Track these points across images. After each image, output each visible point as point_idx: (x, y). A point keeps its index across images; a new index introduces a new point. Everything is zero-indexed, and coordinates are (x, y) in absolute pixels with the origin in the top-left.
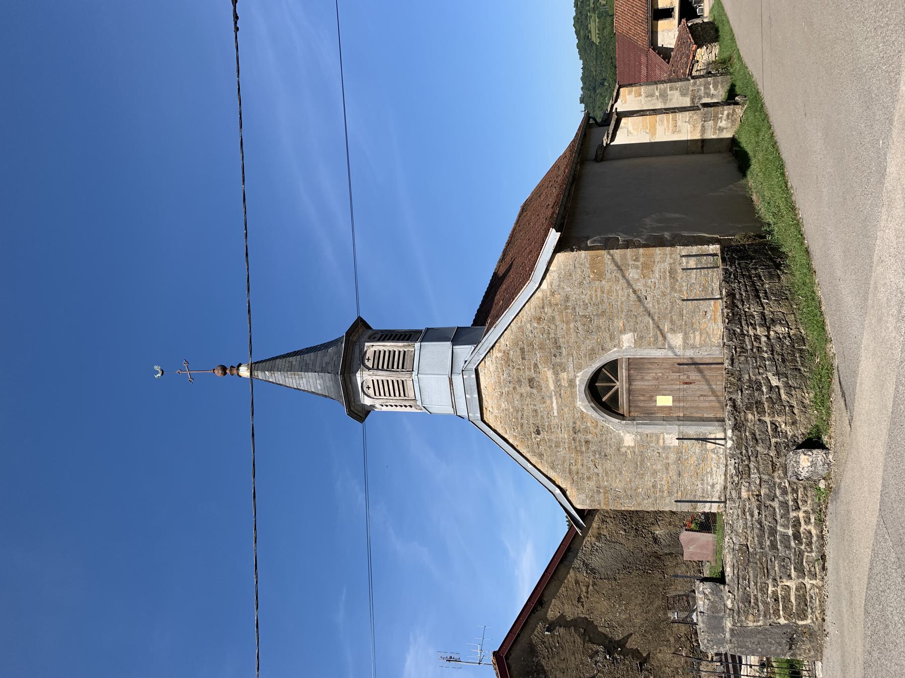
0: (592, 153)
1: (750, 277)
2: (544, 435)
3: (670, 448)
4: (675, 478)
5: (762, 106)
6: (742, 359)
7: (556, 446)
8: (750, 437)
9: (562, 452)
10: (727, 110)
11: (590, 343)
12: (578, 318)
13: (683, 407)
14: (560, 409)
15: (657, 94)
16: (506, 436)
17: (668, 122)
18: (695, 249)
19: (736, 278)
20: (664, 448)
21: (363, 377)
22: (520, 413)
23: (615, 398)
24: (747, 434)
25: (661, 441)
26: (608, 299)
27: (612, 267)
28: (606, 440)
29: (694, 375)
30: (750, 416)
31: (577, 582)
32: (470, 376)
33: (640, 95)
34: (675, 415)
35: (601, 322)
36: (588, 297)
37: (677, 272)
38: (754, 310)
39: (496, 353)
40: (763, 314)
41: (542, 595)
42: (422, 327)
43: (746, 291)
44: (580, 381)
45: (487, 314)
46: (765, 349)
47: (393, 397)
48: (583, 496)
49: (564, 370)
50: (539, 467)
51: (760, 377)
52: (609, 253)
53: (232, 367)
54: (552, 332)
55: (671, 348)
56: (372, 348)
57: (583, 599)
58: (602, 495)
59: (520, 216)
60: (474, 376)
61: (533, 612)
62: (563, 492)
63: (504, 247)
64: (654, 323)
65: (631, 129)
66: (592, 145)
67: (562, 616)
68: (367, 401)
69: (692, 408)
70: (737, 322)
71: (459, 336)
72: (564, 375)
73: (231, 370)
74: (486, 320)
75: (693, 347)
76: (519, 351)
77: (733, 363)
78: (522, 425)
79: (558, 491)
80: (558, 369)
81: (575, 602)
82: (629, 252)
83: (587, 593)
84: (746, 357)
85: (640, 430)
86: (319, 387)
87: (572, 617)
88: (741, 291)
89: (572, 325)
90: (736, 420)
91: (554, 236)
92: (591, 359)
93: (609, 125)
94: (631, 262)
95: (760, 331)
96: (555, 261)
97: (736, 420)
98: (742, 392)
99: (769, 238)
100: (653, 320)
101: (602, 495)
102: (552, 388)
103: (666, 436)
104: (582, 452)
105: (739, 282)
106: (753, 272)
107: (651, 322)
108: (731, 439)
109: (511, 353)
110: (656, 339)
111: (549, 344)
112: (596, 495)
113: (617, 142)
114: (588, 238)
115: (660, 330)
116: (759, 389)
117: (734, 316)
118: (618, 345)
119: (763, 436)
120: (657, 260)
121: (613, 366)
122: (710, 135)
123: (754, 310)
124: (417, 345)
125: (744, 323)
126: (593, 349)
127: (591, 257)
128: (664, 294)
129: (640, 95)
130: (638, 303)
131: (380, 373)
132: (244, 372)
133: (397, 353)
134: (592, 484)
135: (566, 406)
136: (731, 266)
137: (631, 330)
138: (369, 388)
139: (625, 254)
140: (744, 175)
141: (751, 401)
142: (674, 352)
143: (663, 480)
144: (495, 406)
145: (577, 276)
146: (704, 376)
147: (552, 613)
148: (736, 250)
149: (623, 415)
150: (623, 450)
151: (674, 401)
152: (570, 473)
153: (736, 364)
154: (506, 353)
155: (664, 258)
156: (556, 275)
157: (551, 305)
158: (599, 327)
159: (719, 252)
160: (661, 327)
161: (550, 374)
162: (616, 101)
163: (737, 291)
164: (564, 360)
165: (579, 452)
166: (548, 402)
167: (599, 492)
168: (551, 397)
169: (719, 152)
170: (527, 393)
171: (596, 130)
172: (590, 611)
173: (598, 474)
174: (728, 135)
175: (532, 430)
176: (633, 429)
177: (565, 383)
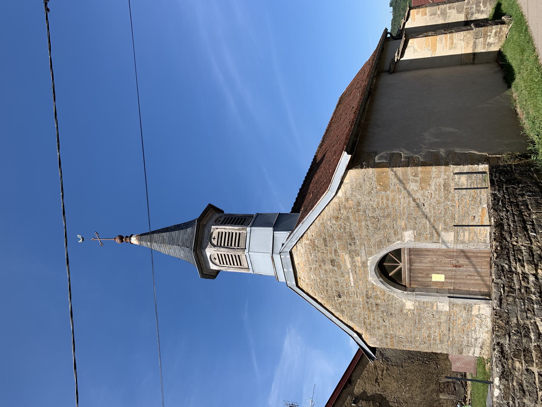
0: (387, 66)
1: (517, 205)
3: (442, 312)
4: (446, 332)
5: (526, 30)
6: (510, 299)
7: (353, 306)
8: (517, 387)
9: (358, 310)
10: (495, 29)
11: (378, 237)
12: (368, 218)
13: (454, 283)
14: (356, 282)
15: (439, 12)
16: (316, 297)
17: (446, 40)
18: (466, 168)
19: (504, 204)
20: (437, 312)
21: (209, 252)
23: (399, 273)
24: (515, 384)
25: (435, 307)
26: (392, 205)
27: (395, 181)
28: (392, 304)
29: (463, 261)
30: (517, 365)
31: (375, 367)
32: (286, 256)
33: (426, 15)
34: (446, 288)
35: (387, 221)
36: (375, 203)
37: (450, 186)
38: (521, 243)
39: (304, 241)
40: (530, 250)
41: (351, 376)
42: (254, 212)
43: (514, 222)
44: (371, 263)
45: (303, 202)
46: (533, 290)
47: (233, 266)
48: (375, 339)
49: (358, 255)
50: (341, 319)
51: (528, 322)
52: (392, 170)
53: (127, 237)
54: (347, 227)
55: (444, 242)
56: (216, 230)
57: (380, 381)
58: (389, 339)
59: (337, 107)
60: (289, 256)
61: (344, 388)
62: (360, 335)
63: (324, 134)
64: (430, 224)
65: (416, 47)
66: (385, 62)
67: (364, 392)
68: (213, 267)
69: (461, 283)
70: (505, 257)
71: (281, 223)
72: (358, 258)
73: (125, 239)
74: (301, 208)
75: (463, 242)
76: (322, 240)
77: (501, 303)
78: (327, 291)
79: (355, 335)
80: (353, 254)
81: (374, 382)
82: (410, 170)
83: (382, 375)
84: (514, 298)
85: (418, 299)
86: (182, 256)
87: (371, 393)
88: (510, 223)
89: (363, 223)
90: (503, 367)
91: (346, 158)
92: (379, 248)
93: (401, 38)
94: (411, 178)
95: (528, 269)
96: (348, 176)
97: (503, 367)
98: (510, 336)
99: (533, 158)
100: (430, 221)
101: (389, 339)
102: (349, 267)
103: (439, 304)
104: (373, 311)
105: (507, 211)
106: (520, 199)
107: (428, 223)
108: (499, 387)
109: (317, 241)
110: (432, 235)
111: (346, 236)
113: (405, 58)
114: (376, 153)
115: (436, 229)
116: (527, 336)
117: (500, 231)
118: (401, 239)
119: (531, 388)
120: (433, 176)
121: (398, 253)
122: (480, 49)
123: (521, 243)
124: (248, 229)
125: (512, 258)
126: (380, 241)
127: (378, 172)
128: (439, 202)
129: (426, 15)
130: (417, 209)
131: (222, 249)
132: (134, 240)
133: (234, 234)
134: (381, 332)
135: (360, 280)
136: (499, 191)
137: (411, 229)
138: (215, 259)
139: (406, 172)
140: (509, 87)
141: (519, 348)
142: (446, 246)
143: (436, 333)
144: (306, 277)
145: (366, 187)
146: (471, 262)
147: (357, 390)
148: (503, 171)
149: (405, 286)
150: (405, 311)
151: (445, 278)
152: (364, 324)
153: (504, 305)
154: (313, 242)
155: (438, 174)
156: (349, 186)
157: (345, 208)
158: (385, 226)
159: (487, 171)
160: (436, 227)
161: (347, 257)
162: (407, 20)
163: (505, 221)
164: (357, 248)
166: (346, 276)
167: (386, 337)
168: (348, 273)
169: (488, 63)
170: (330, 269)
171: (393, 43)
172: (384, 389)
173: (385, 326)
174: (495, 48)
176: (414, 298)
177: (359, 264)
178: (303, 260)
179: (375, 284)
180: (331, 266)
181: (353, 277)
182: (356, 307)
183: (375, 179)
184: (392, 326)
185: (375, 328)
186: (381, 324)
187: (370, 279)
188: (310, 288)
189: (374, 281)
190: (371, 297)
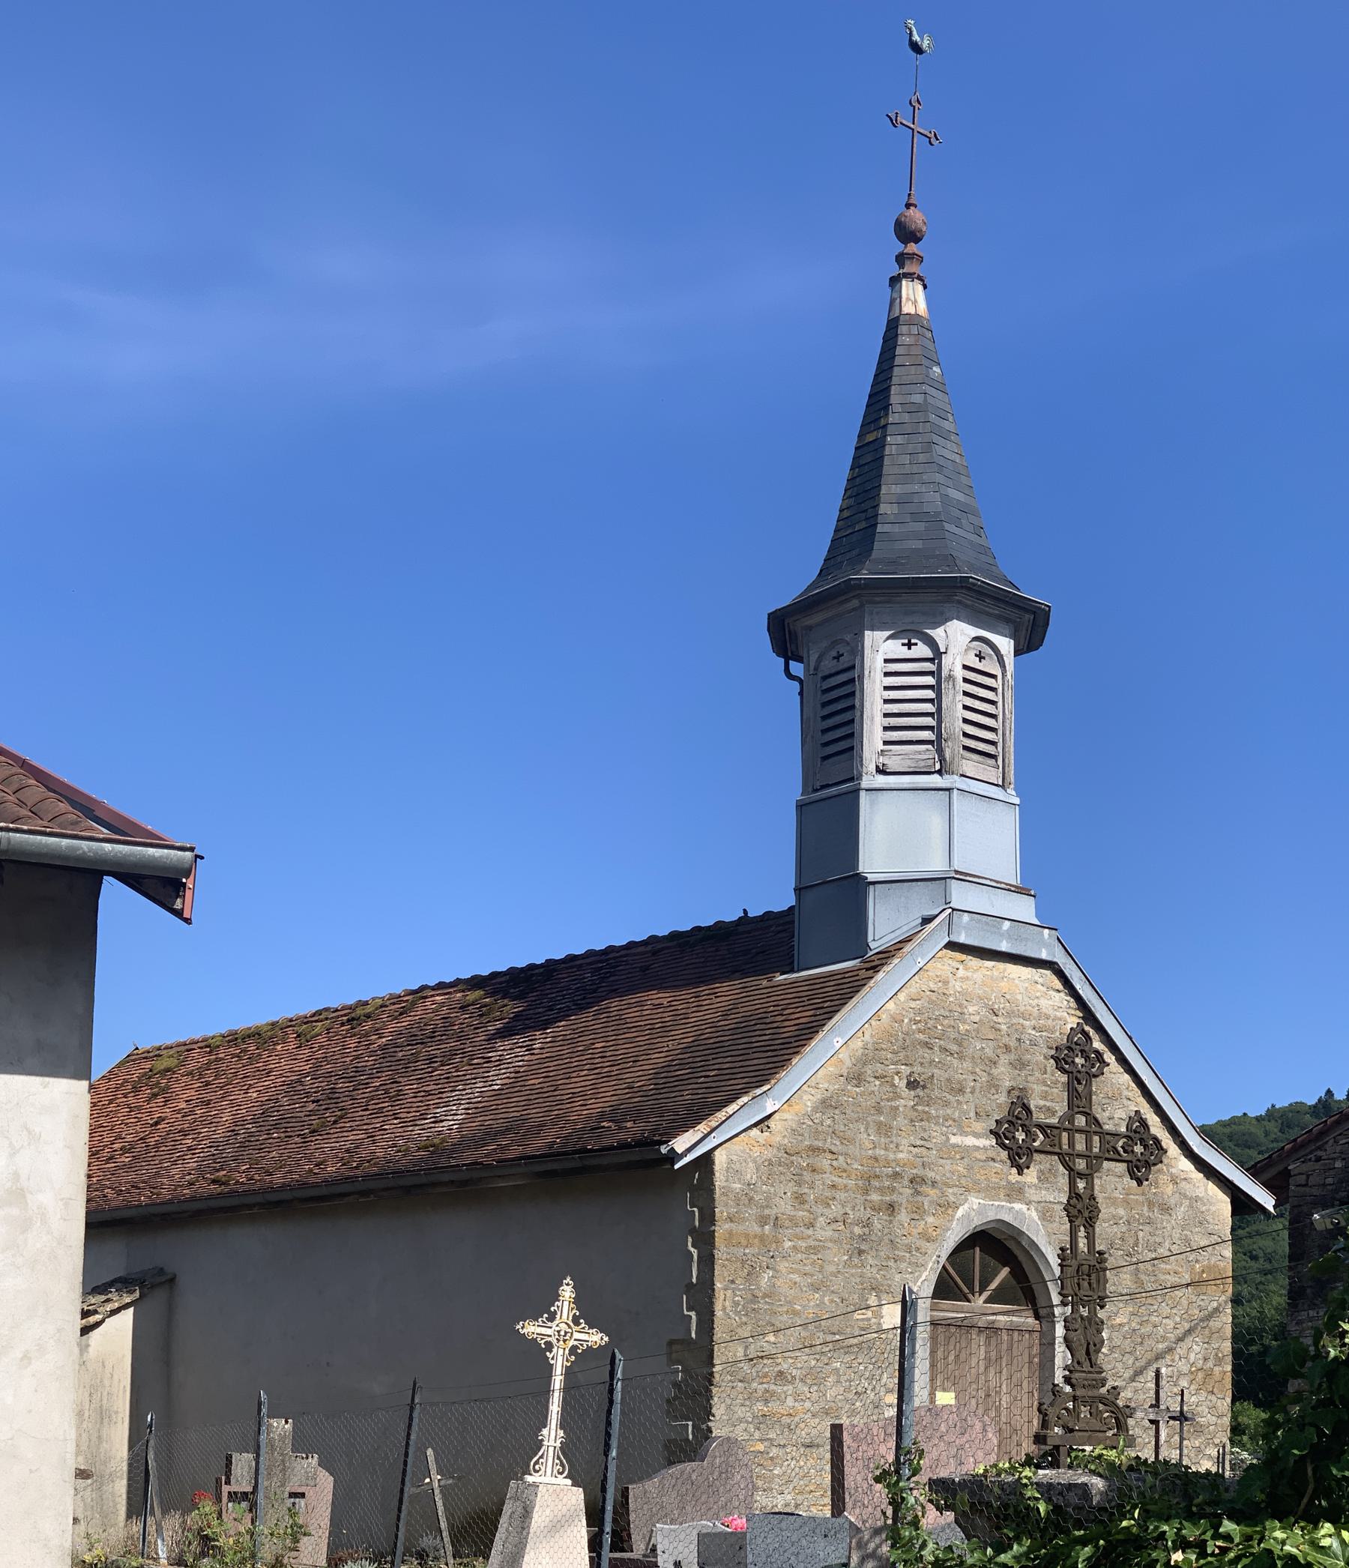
2: (906, 1099)
7: (879, 1124)
9: (866, 1139)
22: (954, 1048)
48: (750, 1175)
89: (1121, 1212)
101: (757, 1229)
104: (866, 1192)
112: (754, 1211)
135: (969, 1168)
152: (814, 1150)
165: (868, 1181)
173: (812, 1225)
175: (917, 1069)
178: (1019, 997)
179: (960, 1213)
180: (1007, 1084)
181: (978, 1148)
182: (879, 1132)
183: (1213, 1260)
184: (814, 1250)
185: (799, 1184)
186: (819, 1209)
187: (974, 1201)
188: (932, 986)
189: (966, 1216)
190: (918, 1193)
